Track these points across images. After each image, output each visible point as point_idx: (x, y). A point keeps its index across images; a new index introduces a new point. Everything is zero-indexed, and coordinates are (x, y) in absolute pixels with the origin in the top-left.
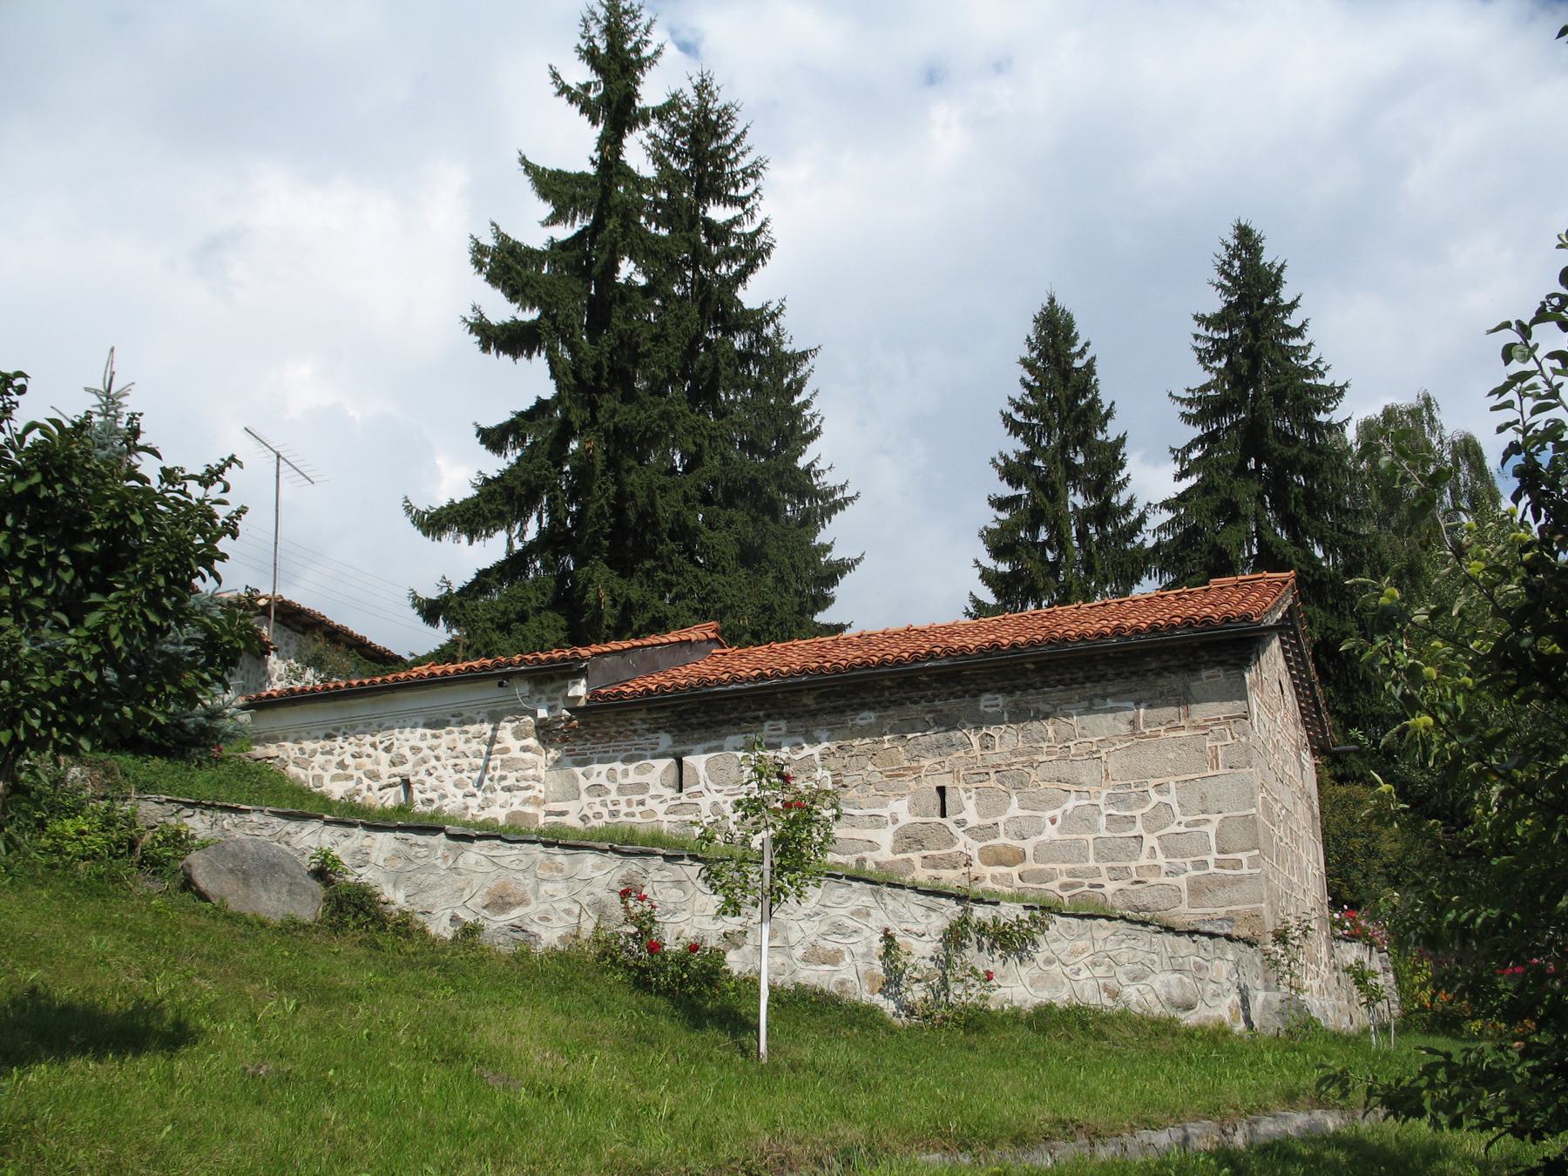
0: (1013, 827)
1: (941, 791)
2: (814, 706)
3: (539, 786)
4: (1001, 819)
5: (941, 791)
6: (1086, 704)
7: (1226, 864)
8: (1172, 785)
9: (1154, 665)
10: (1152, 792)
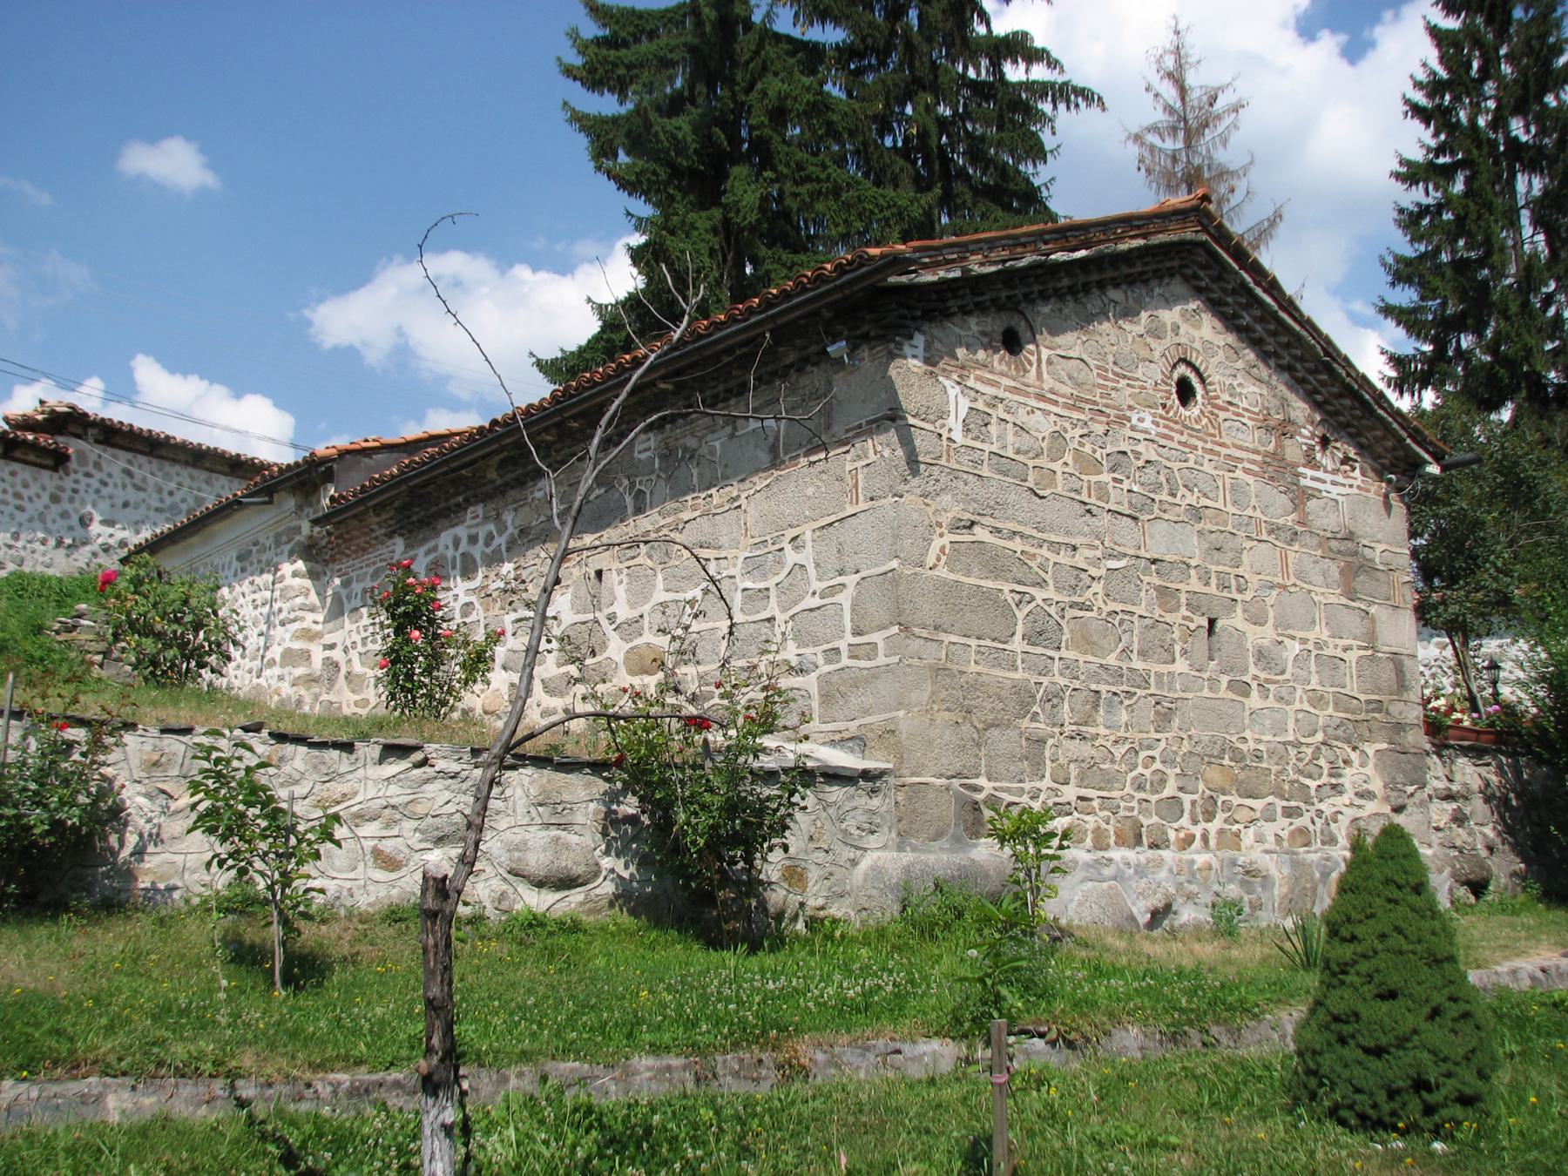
0: (658, 618)
1: (599, 574)
2: (499, 481)
3: (310, 617)
4: (646, 609)
5: (599, 574)
6: (729, 429)
7: (862, 651)
8: (808, 536)
9: (791, 358)
10: (788, 548)
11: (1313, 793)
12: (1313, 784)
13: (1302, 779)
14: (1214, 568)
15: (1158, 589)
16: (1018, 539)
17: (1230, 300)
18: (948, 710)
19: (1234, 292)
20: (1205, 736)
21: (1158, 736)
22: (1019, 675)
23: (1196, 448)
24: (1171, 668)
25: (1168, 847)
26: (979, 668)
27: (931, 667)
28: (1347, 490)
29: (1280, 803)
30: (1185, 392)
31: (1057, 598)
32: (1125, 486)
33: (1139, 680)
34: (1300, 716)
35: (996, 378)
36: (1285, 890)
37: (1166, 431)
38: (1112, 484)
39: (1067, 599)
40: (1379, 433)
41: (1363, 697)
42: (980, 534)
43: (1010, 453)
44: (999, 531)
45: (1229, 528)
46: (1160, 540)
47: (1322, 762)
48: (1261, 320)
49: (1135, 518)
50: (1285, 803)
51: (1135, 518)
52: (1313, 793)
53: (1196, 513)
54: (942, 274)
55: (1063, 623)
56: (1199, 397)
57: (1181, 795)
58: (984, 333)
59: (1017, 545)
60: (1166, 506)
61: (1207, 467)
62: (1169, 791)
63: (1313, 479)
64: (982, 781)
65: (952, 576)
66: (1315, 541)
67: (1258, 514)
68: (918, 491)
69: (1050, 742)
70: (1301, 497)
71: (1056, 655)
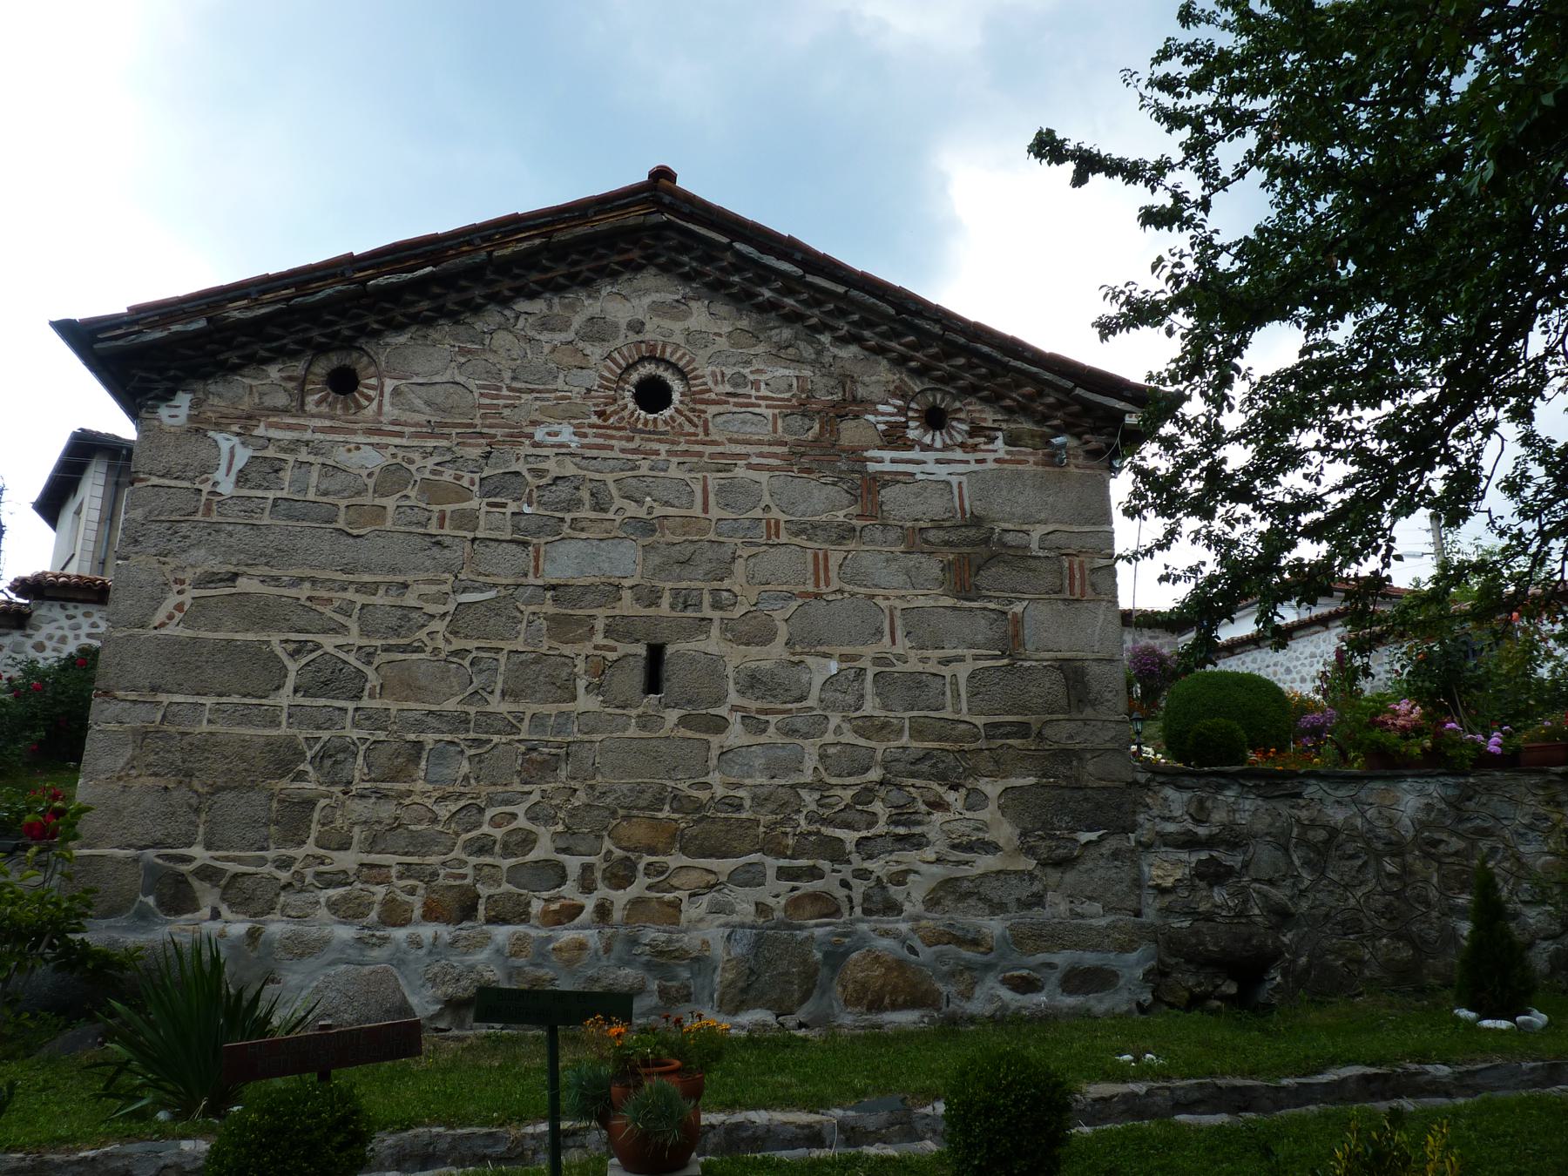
11: (850, 847)
12: (849, 837)
13: (828, 831)
14: (669, 585)
15: (550, 618)
16: (307, 585)
17: (736, 279)
18: (156, 774)
19: (736, 269)
20: (623, 784)
21: (527, 788)
22: (284, 730)
23: (657, 453)
24: (565, 707)
25: (523, 921)
26: (213, 728)
27: (135, 731)
28: (961, 468)
29: (772, 863)
30: (653, 395)
31: (364, 642)
32: (512, 507)
33: (500, 725)
34: (831, 751)
35: (301, 421)
36: (730, 976)
37: (600, 441)
38: (485, 508)
39: (379, 643)
40: (1028, 390)
41: (980, 721)
42: (243, 584)
43: (311, 496)
44: (277, 579)
45: (712, 536)
46: (565, 562)
47: (877, 807)
48: (788, 291)
49: (525, 544)
50: (783, 862)
51: (525, 544)
52: (850, 847)
53: (646, 527)
54: (175, 328)
55: (369, 672)
56: (676, 397)
57: (562, 857)
58: (290, 379)
59: (305, 591)
60: (584, 524)
61: (674, 472)
62: (543, 850)
63: (893, 461)
64: (199, 853)
65: (189, 633)
66: (892, 535)
67: (775, 513)
68: (153, 551)
69: (322, 802)
70: (868, 488)
71: (351, 705)
